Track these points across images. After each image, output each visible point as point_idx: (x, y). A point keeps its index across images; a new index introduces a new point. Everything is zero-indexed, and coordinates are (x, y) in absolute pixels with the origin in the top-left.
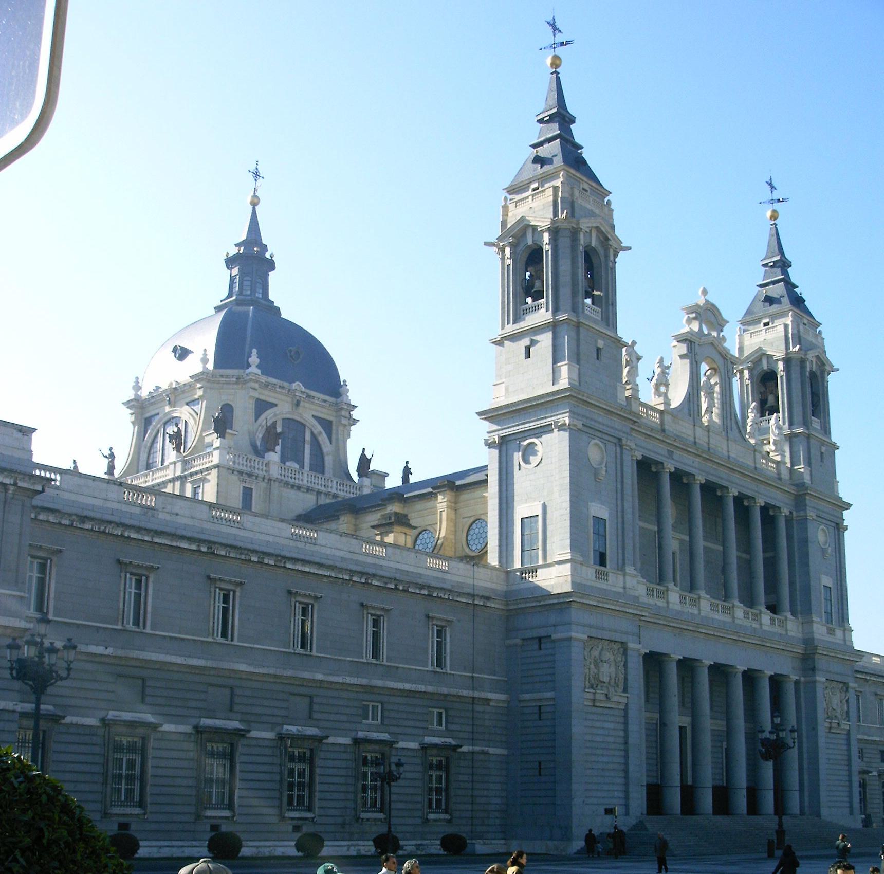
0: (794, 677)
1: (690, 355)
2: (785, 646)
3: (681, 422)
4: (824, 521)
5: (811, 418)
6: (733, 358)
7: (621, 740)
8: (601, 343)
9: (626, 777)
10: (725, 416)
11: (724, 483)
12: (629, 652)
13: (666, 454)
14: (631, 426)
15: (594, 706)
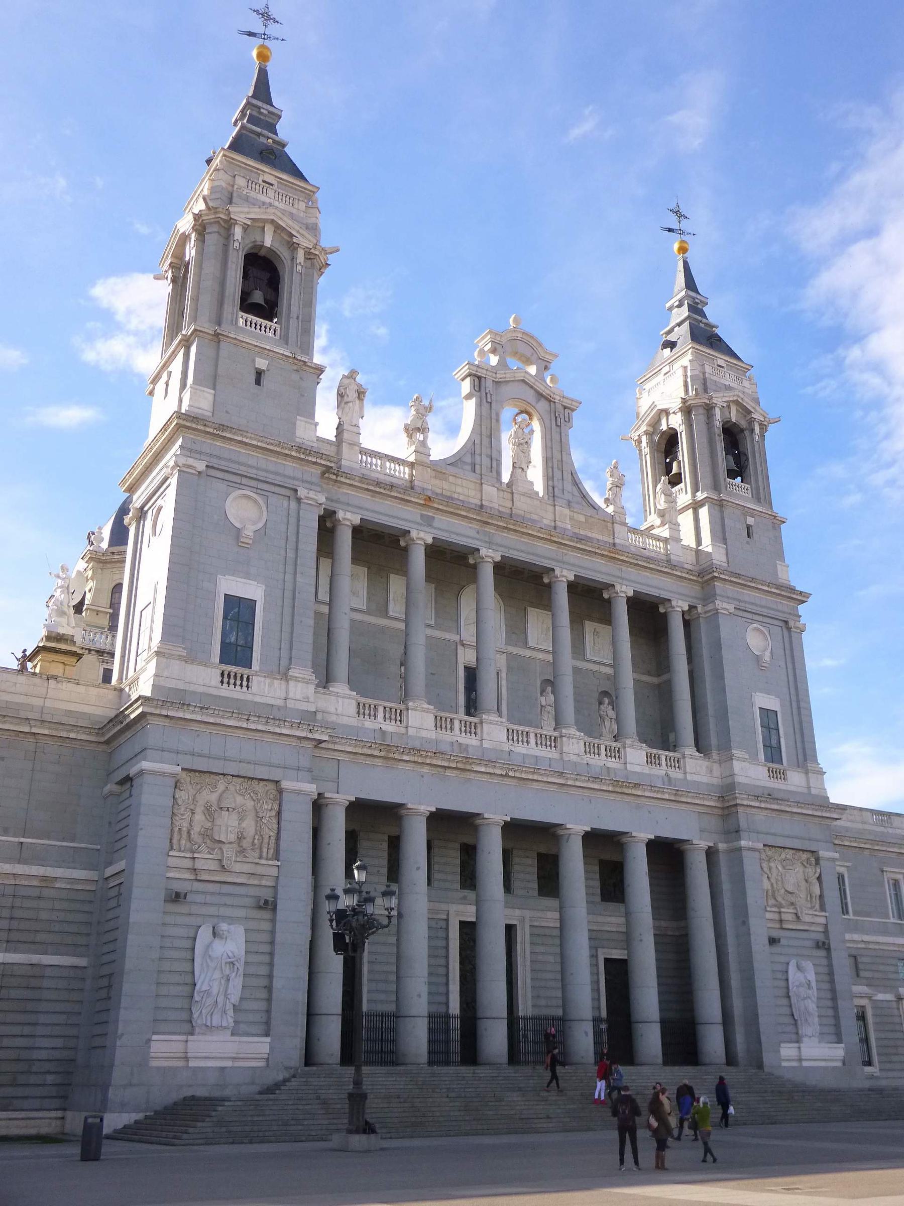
0: (704, 844)
1: (478, 394)
2: (676, 795)
3: (451, 479)
4: (756, 617)
5: (725, 481)
6: (565, 400)
7: (265, 937)
8: (261, 363)
9: (269, 1000)
10: (550, 474)
11: (547, 563)
12: (285, 795)
13: (419, 520)
14: (334, 477)
15: (197, 880)
